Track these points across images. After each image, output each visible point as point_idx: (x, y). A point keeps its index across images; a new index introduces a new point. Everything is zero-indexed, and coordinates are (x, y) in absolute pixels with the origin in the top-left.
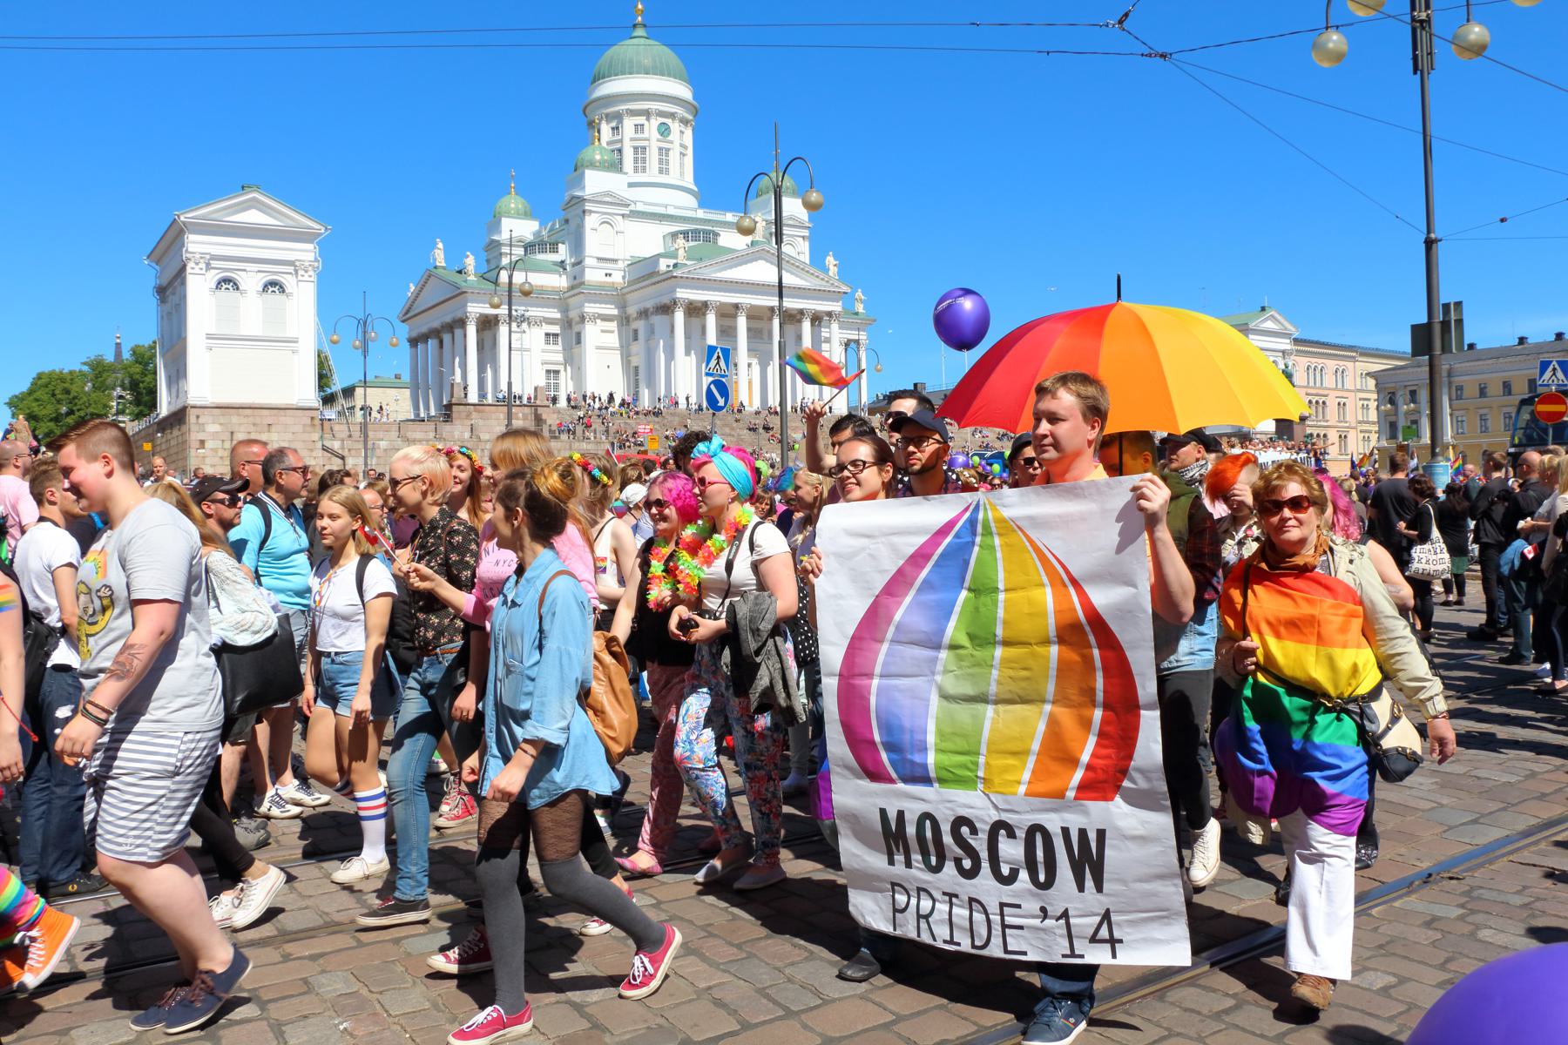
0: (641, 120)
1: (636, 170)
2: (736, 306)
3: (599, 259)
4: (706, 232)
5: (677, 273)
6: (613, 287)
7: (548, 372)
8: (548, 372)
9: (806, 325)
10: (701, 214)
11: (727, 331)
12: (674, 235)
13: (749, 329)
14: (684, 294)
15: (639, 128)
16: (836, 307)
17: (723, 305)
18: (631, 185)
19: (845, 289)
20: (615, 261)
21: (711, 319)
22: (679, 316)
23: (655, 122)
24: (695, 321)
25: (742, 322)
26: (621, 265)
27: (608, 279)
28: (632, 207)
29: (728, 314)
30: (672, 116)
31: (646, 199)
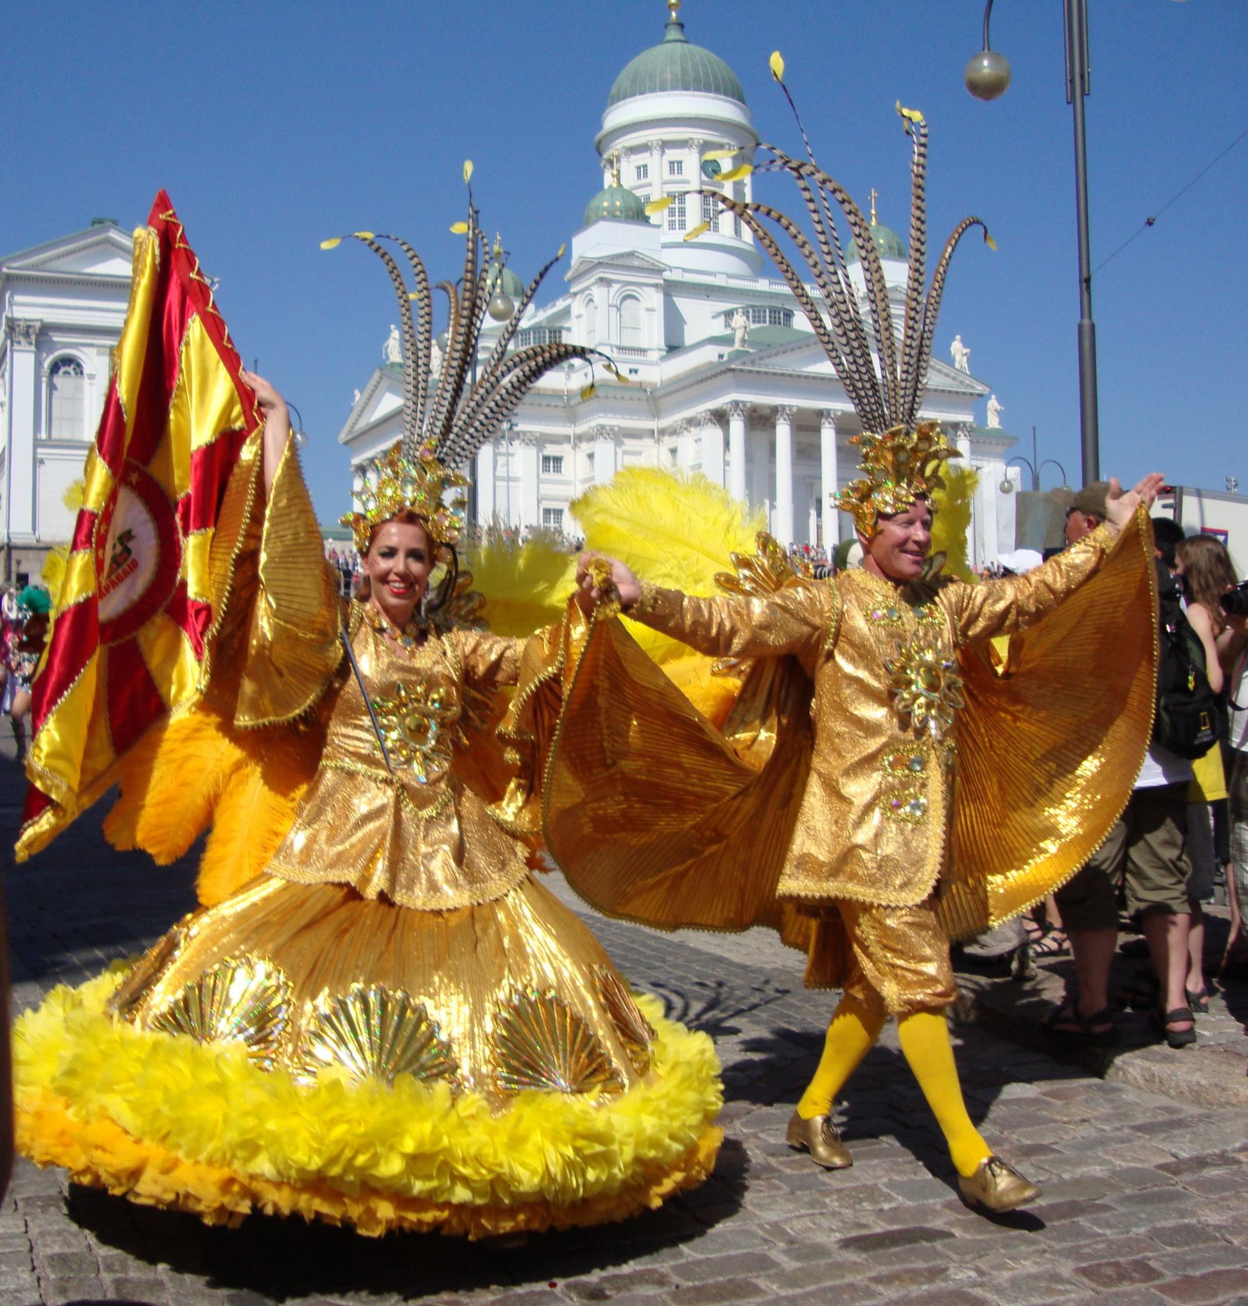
1: (672, 225)
4: (774, 311)
6: (641, 387)
8: (547, 512)
10: (763, 285)
11: (806, 453)
12: (729, 314)
16: (968, 418)
17: (801, 411)
18: (665, 246)
19: (980, 388)
20: (643, 351)
21: (783, 431)
24: (761, 436)
28: (667, 275)
31: (684, 263)
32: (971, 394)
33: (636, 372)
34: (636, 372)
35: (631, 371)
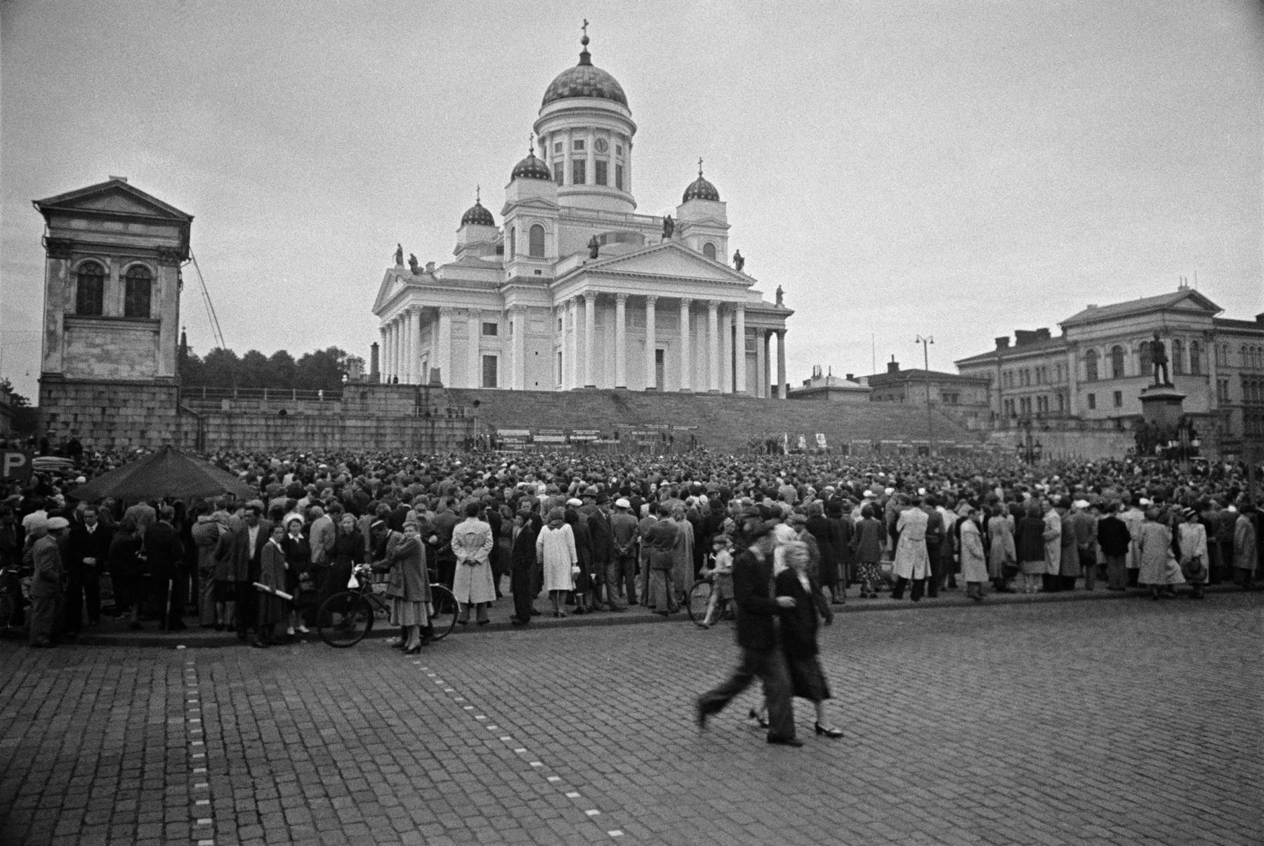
0: (578, 136)
25: (651, 311)
30: (608, 131)
33: (539, 272)
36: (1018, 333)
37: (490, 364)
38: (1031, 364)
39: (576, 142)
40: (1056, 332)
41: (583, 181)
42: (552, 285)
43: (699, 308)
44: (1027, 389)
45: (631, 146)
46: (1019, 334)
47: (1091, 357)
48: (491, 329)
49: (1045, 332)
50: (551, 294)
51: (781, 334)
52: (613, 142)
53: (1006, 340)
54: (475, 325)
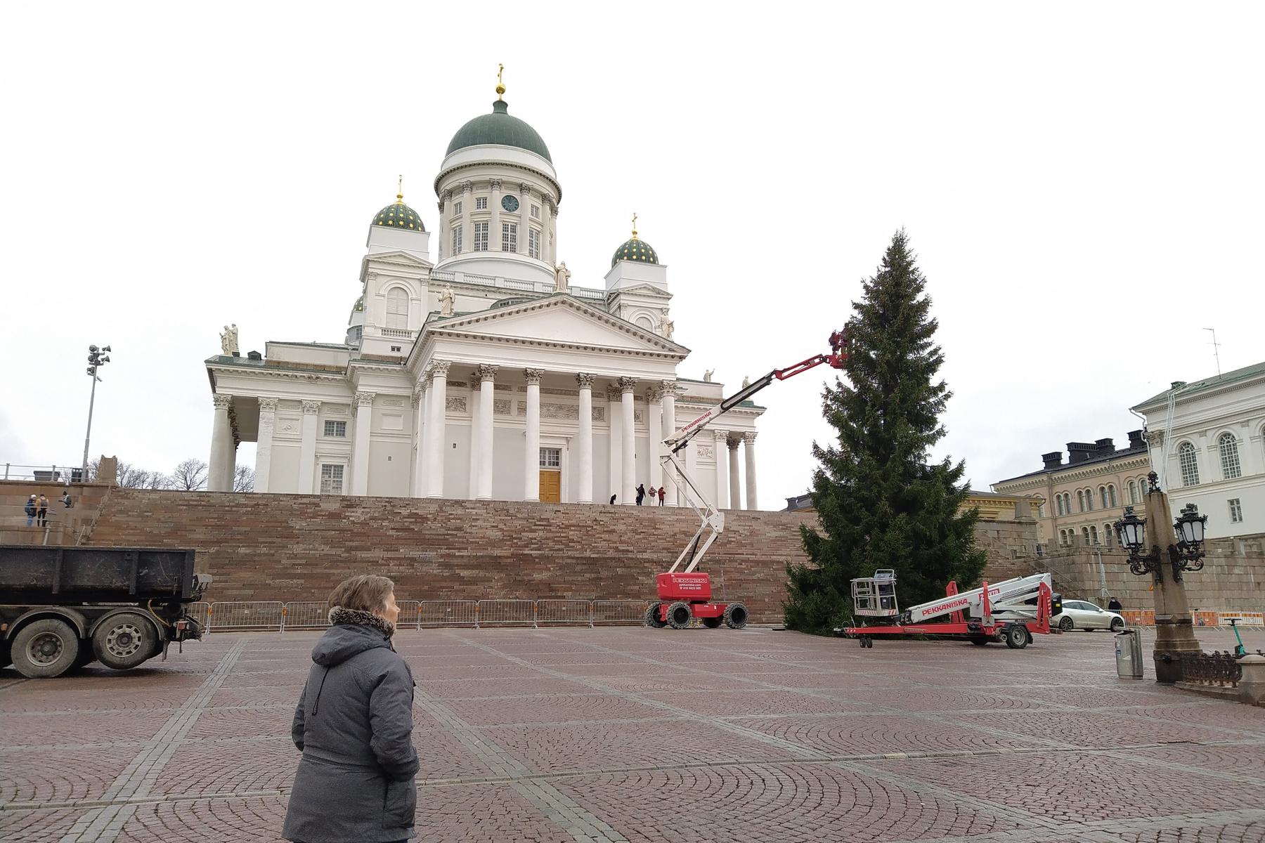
0: (481, 193)
2: (527, 374)
3: (384, 331)
5: (436, 327)
7: (326, 468)
8: (326, 468)
9: (628, 397)
13: (542, 405)
14: (446, 353)
15: (482, 202)
20: (409, 333)
22: (440, 383)
23: (497, 196)
25: (534, 391)
26: (414, 337)
27: (395, 354)
29: (511, 383)
30: (522, 188)
32: (673, 357)
34: (399, 349)
35: (393, 349)
36: (1073, 447)
37: (333, 472)
38: (1093, 484)
39: (478, 200)
40: (1122, 443)
41: (485, 248)
42: (409, 364)
43: (610, 390)
44: (1092, 516)
45: (554, 211)
46: (1073, 447)
47: (1187, 454)
48: (335, 428)
49: (1104, 446)
50: (410, 376)
51: (749, 438)
52: (527, 201)
53: (1057, 456)
54: (311, 425)
